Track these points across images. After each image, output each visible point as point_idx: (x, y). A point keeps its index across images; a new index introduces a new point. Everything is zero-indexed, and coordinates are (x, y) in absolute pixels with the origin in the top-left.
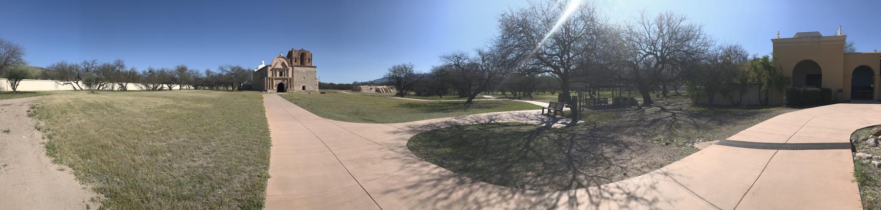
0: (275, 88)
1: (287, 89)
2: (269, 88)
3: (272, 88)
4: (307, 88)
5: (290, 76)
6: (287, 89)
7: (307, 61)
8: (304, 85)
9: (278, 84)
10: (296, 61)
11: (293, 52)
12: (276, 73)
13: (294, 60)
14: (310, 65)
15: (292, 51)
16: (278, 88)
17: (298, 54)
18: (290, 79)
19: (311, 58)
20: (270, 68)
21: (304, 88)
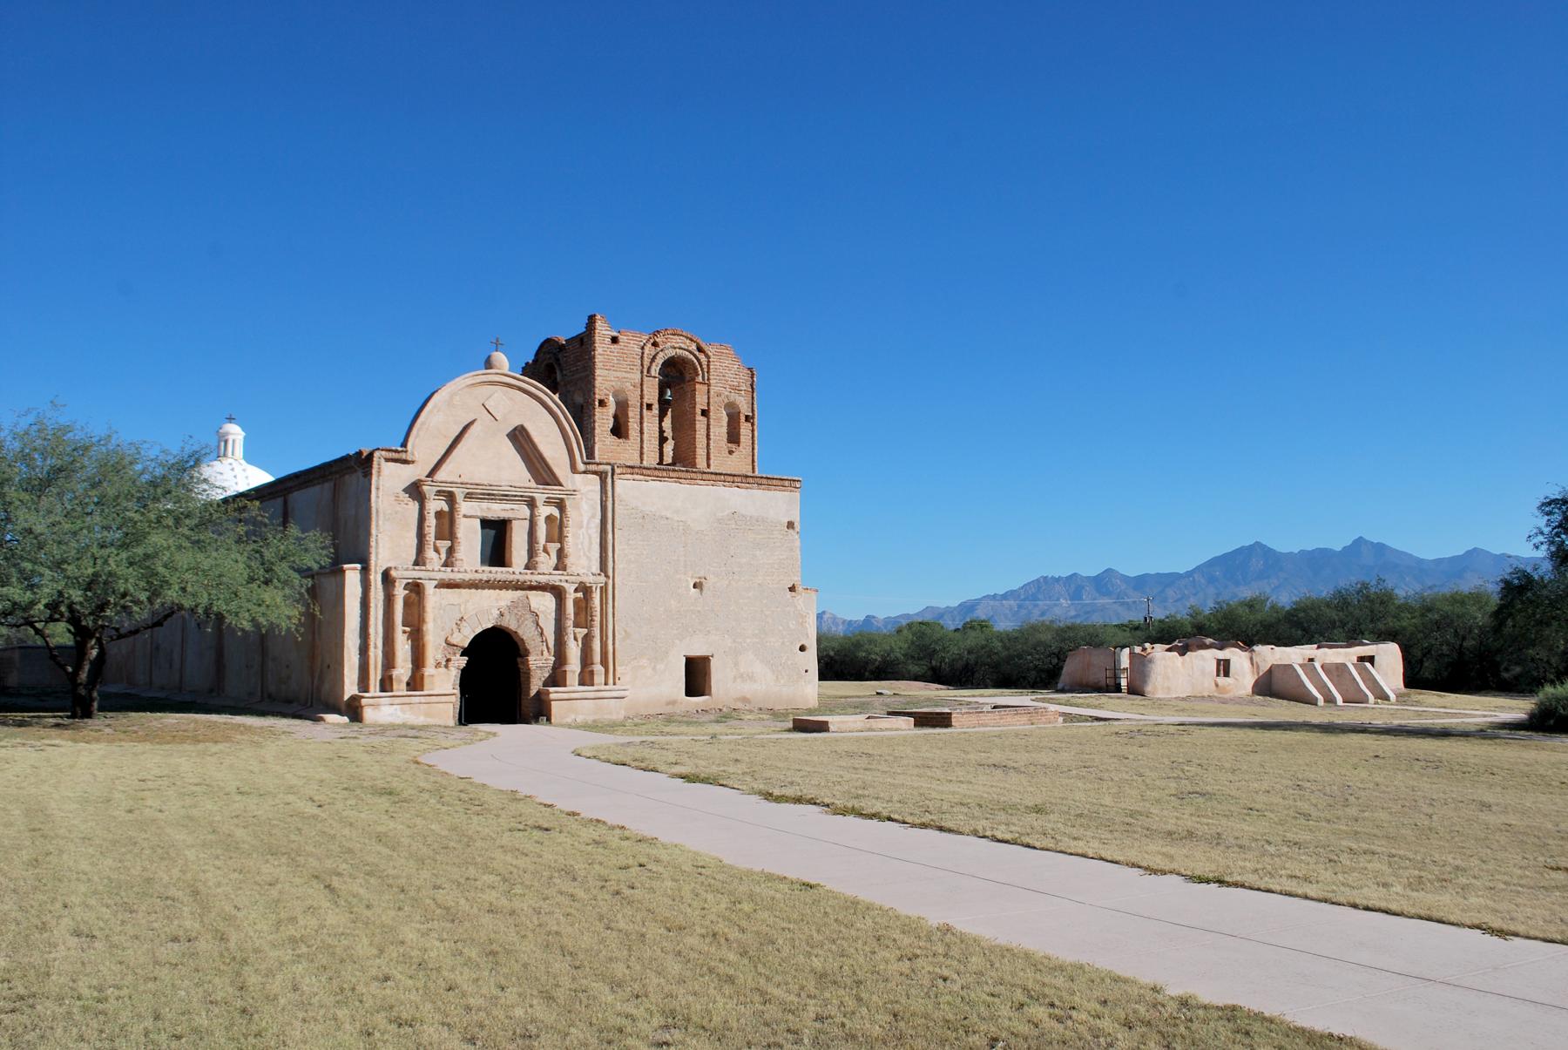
0: (445, 681)
1: (554, 693)
2: (386, 684)
3: (415, 683)
4: (719, 677)
5: (583, 562)
6: (554, 693)
7: (720, 429)
8: (696, 652)
9: (465, 638)
10: (619, 430)
11: (602, 348)
12: (447, 526)
13: (603, 420)
14: (738, 462)
15: (584, 341)
16: (468, 681)
17: (645, 372)
18: (585, 589)
19: (745, 410)
20: (388, 481)
21: (697, 676)
